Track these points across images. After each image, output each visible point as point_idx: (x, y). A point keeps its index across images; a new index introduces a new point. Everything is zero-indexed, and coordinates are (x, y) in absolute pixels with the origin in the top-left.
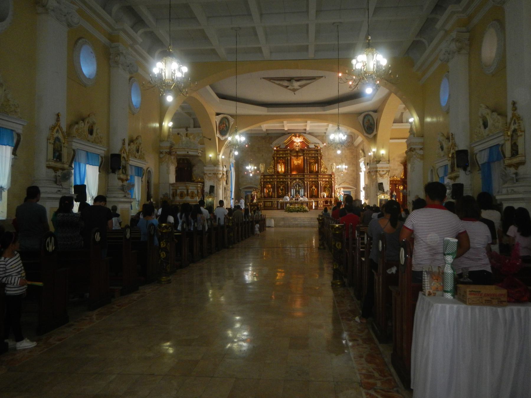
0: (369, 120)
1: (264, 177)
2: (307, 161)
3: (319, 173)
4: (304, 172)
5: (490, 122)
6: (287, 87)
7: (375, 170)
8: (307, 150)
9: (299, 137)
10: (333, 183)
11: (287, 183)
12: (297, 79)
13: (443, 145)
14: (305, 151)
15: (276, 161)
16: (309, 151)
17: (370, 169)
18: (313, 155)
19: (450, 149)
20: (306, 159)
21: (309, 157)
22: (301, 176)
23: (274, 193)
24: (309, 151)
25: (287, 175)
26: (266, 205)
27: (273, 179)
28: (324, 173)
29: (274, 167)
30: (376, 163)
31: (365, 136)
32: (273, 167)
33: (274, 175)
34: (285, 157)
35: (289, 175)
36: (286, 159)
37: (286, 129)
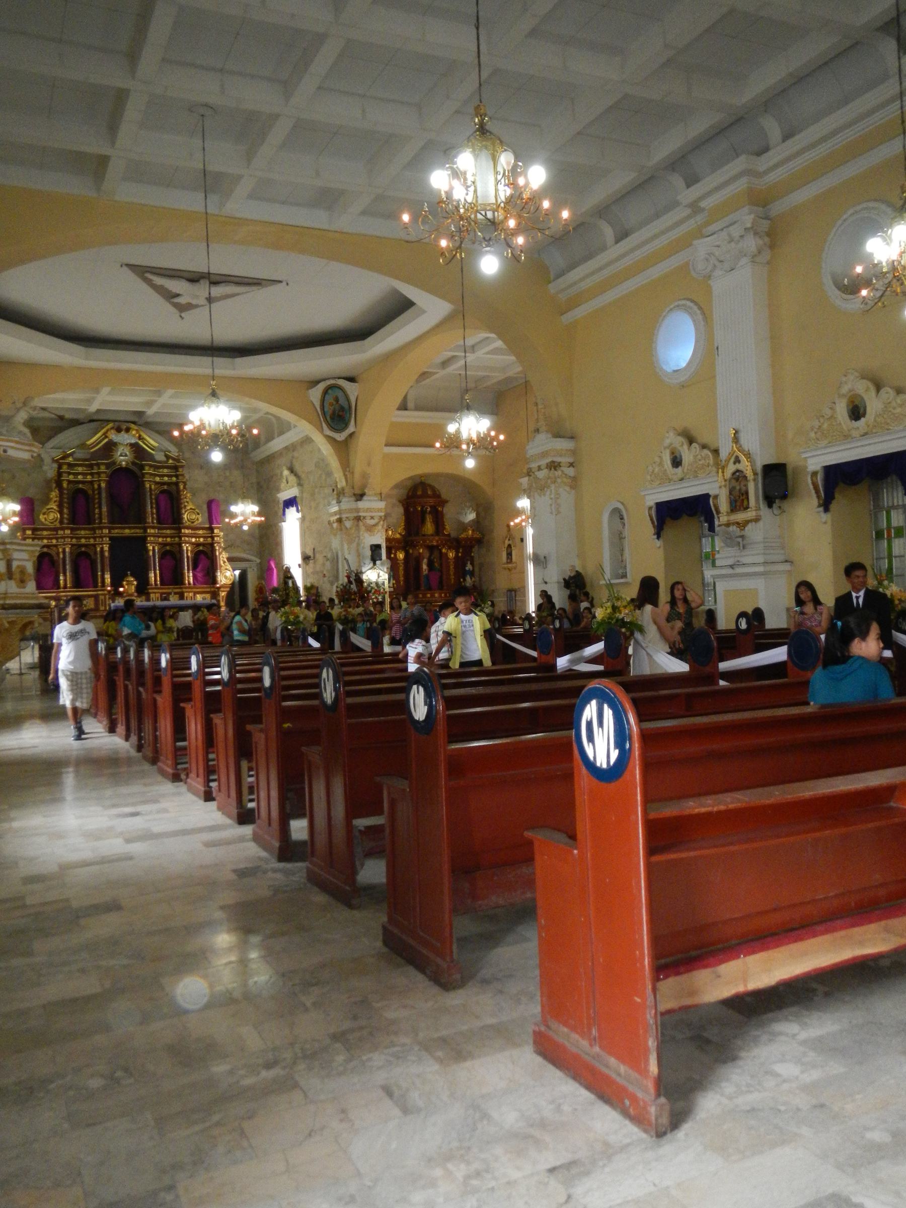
0: (337, 399)
1: (33, 534)
2: (151, 495)
5: (873, 405)
6: (178, 295)
7: (356, 515)
8: (151, 466)
9: (128, 430)
10: (217, 548)
12: (218, 278)
13: (681, 456)
14: (147, 468)
16: (156, 468)
17: (340, 512)
18: (166, 479)
19: (728, 461)
21: (157, 483)
22: (138, 531)
24: (156, 468)
25: (101, 528)
27: (62, 538)
28: (193, 523)
29: (60, 506)
30: (353, 499)
31: (328, 437)
32: (55, 507)
33: (63, 529)
34: (91, 482)
35: (105, 528)
36: (96, 486)
37: (93, 408)
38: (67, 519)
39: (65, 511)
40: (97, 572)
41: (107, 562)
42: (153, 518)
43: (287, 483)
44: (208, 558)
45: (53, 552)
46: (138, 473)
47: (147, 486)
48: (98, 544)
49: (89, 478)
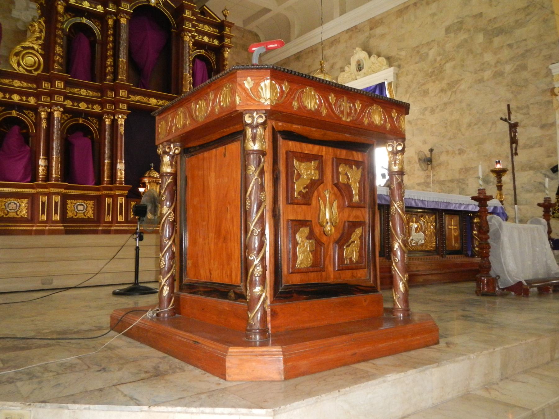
11: (108, 122)
14: (188, 14)
15: (60, 18)
18: (206, 39)
20: (187, 45)
23: (48, 157)
25: (115, 89)
33: (51, 80)
34: (101, 18)
35: (124, 87)
36: (110, 22)
38: (60, 65)
39: (58, 49)
40: (104, 160)
41: (121, 143)
43: (360, 68)
45: (28, 118)
46: (173, 21)
47: (187, 38)
48: (108, 113)
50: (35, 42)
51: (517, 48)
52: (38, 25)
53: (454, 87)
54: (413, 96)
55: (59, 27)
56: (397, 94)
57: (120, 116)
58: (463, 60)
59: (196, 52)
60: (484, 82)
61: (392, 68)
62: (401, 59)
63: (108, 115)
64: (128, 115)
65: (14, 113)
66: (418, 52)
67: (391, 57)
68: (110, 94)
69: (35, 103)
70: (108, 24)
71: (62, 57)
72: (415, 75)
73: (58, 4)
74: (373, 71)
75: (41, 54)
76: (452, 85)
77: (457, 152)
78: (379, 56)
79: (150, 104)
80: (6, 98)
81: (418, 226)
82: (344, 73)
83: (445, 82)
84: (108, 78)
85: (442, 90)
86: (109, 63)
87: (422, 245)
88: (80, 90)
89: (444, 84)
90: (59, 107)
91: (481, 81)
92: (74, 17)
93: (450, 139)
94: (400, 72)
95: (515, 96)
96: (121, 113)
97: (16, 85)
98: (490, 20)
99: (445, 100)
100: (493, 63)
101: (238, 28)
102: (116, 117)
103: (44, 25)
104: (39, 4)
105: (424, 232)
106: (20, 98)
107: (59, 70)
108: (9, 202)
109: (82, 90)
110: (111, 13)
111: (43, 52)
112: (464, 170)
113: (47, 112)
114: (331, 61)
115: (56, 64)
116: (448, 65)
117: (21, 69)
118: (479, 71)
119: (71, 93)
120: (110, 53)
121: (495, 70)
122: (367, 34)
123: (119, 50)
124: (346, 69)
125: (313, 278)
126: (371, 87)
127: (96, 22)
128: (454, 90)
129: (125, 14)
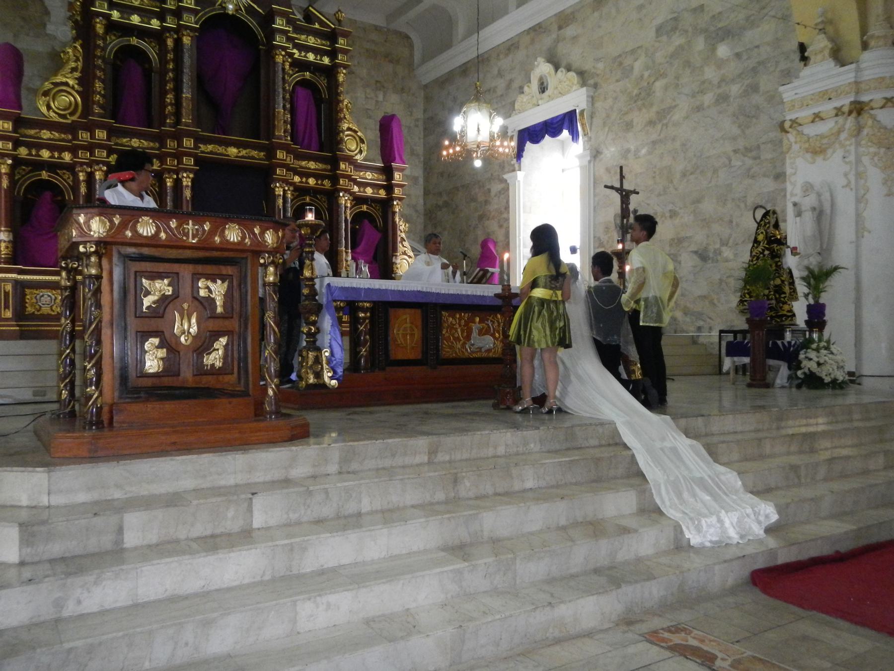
1: (15, 130)
3: (341, 150)
4: (270, 133)
11: (169, 183)
14: (279, 23)
15: (100, 43)
18: (311, 57)
20: (280, 68)
22: (254, 153)
25: (178, 136)
26: (30, 309)
29: (85, 82)
33: (90, 128)
34: (157, 37)
35: (189, 134)
36: (170, 43)
38: (101, 107)
39: (98, 85)
42: (285, 132)
43: (543, 89)
44: (376, 227)
45: (63, 180)
47: (279, 59)
48: (169, 171)
49: (155, 24)
50: (70, 75)
51: (747, 59)
52: (73, 51)
53: (665, 117)
54: (612, 131)
55: (99, 54)
56: (593, 128)
57: (185, 175)
58: (677, 78)
59: (298, 76)
60: (703, 109)
61: (585, 88)
62: (598, 75)
63: (169, 173)
64: (196, 173)
65: (45, 175)
66: (621, 64)
67: (586, 71)
68: (171, 144)
69: (71, 160)
70: (166, 45)
71: (103, 96)
72: (616, 98)
73: (97, 23)
74: (560, 93)
75: (77, 92)
76: (663, 114)
77: (668, 215)
78: (569, 69)
79: (228, 156)
80: (32, 155)
81: (483, 328)
82: (522, 96)
83: (655, 109)
84: (168, 121)
85: (651, 123)
86: (168, 101)
87: (489, 351)
88: (131, 140)
89: (652, 114)
90: (101, 165)
91: (699, 108)
92: (120, 37)
93: (659, 195)
94: (596, 94)
95: (743, 132)
96: (186, 170)
97: (45, 137)
98: (714, 16)
99: (654, 137)
100: (715, 81)
101: (377, 28)
102: (180, 176)
103: (81, 50)
104: (73, 22)
105: (493, 335)
106: (50, 154)
107: (100, 115)
108: (41, 294)
109: (133, 140)
110: (169, 29)
111: (80, 89)
112: (676, 241)
113: (86, 172)
114: (508, 78)
115: (95, 106)
116: (659, 85)
117: (52, 114)
118: (698, 93)
119: (116, 144)
120: (170, 86)
121: (720, 91)
122: (554, 36)
123: (182, 81)
124: (526, 89)
125: (167, 381)
126: (557, 117)
127: (151, 42)
128: (665, 122)
129: (188, 31)
